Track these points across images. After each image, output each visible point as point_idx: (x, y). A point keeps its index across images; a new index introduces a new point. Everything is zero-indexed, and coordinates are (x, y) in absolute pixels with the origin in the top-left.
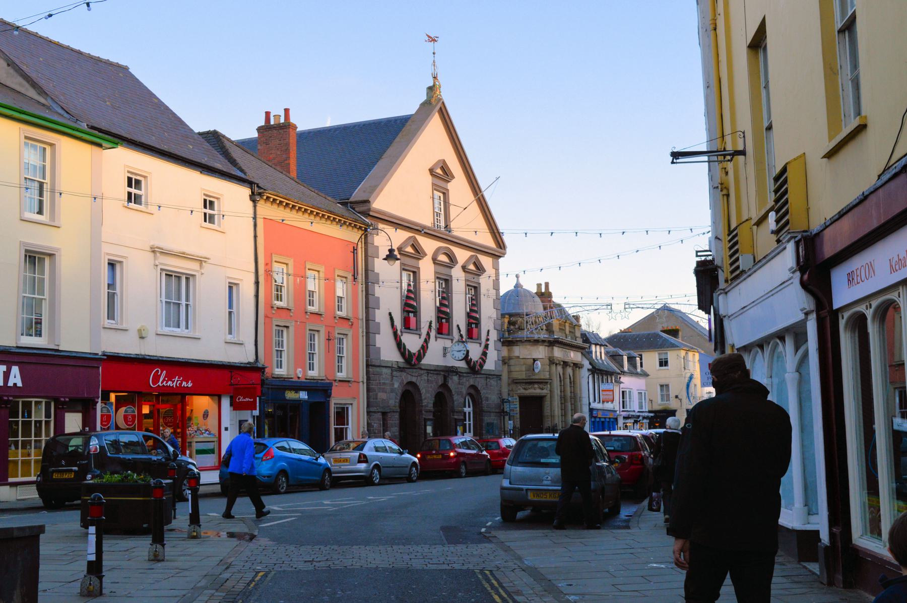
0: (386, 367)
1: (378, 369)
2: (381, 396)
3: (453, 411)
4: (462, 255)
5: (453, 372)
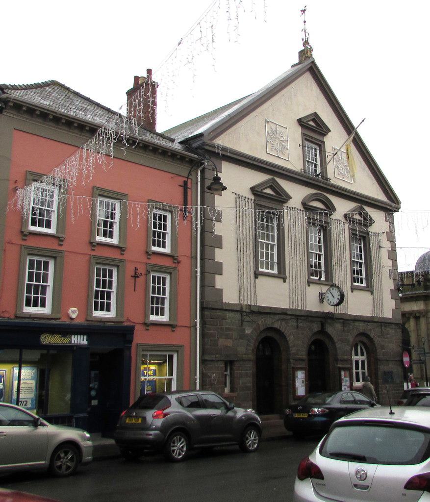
0: (232, 311)
1: (219, 313)
2: (222, 342)
3: (337, 360)
4: (342, 207)
5: (330, 318)
